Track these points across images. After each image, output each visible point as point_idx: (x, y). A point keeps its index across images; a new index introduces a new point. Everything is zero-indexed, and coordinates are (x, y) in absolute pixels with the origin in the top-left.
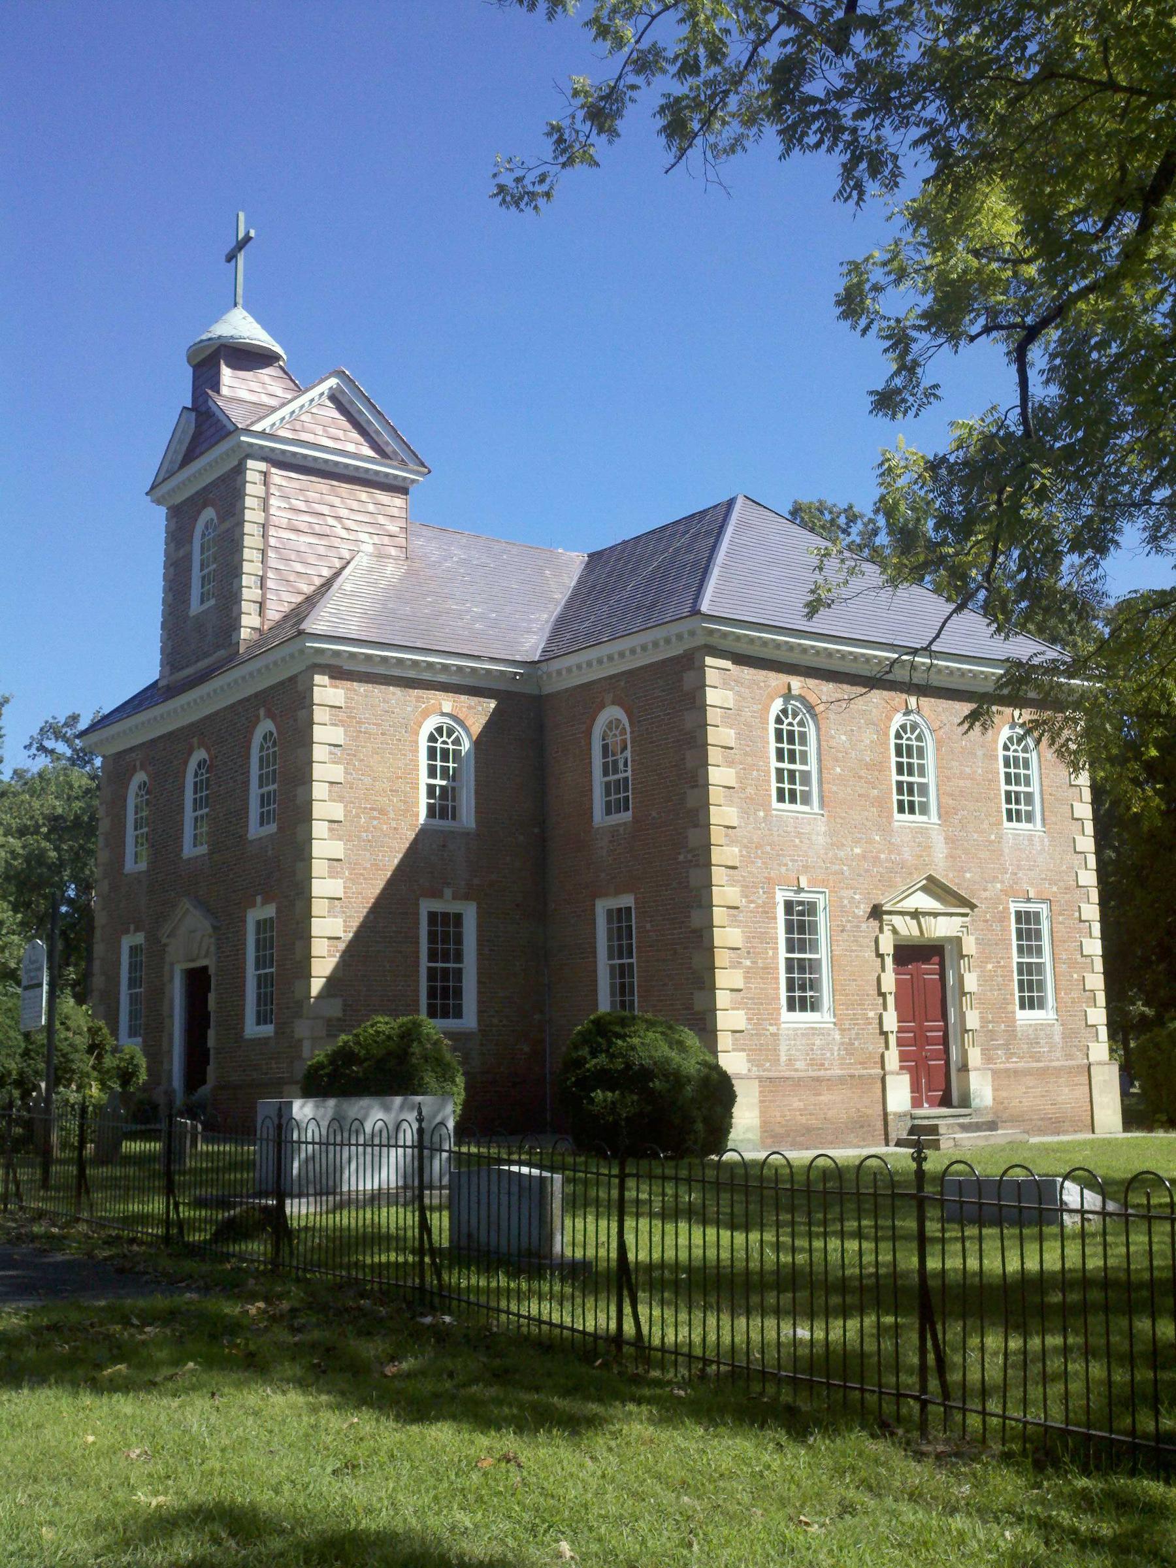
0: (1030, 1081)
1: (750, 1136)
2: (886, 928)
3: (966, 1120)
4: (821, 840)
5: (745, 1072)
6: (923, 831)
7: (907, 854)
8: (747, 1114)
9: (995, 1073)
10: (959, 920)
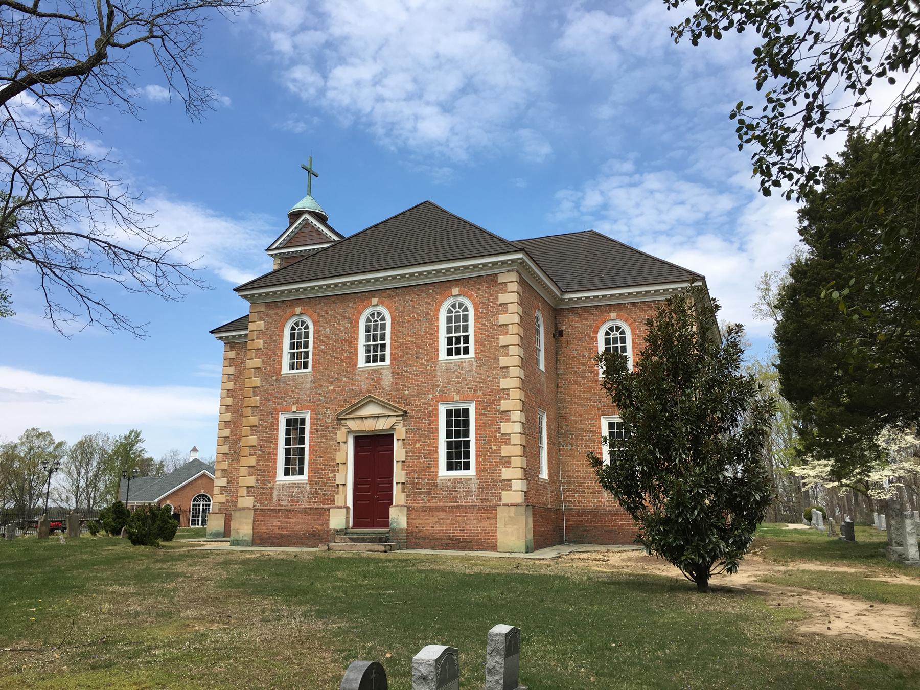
0: (442, 514)
1: (245, 538)
2: (343, 428)
3: (355, 536)
4: (308, 386)
5: (251, 506)
6: (377, 371)
7: (364, 385)
8: (246, 527)
9: (408, 508)
10: (393, 420)
